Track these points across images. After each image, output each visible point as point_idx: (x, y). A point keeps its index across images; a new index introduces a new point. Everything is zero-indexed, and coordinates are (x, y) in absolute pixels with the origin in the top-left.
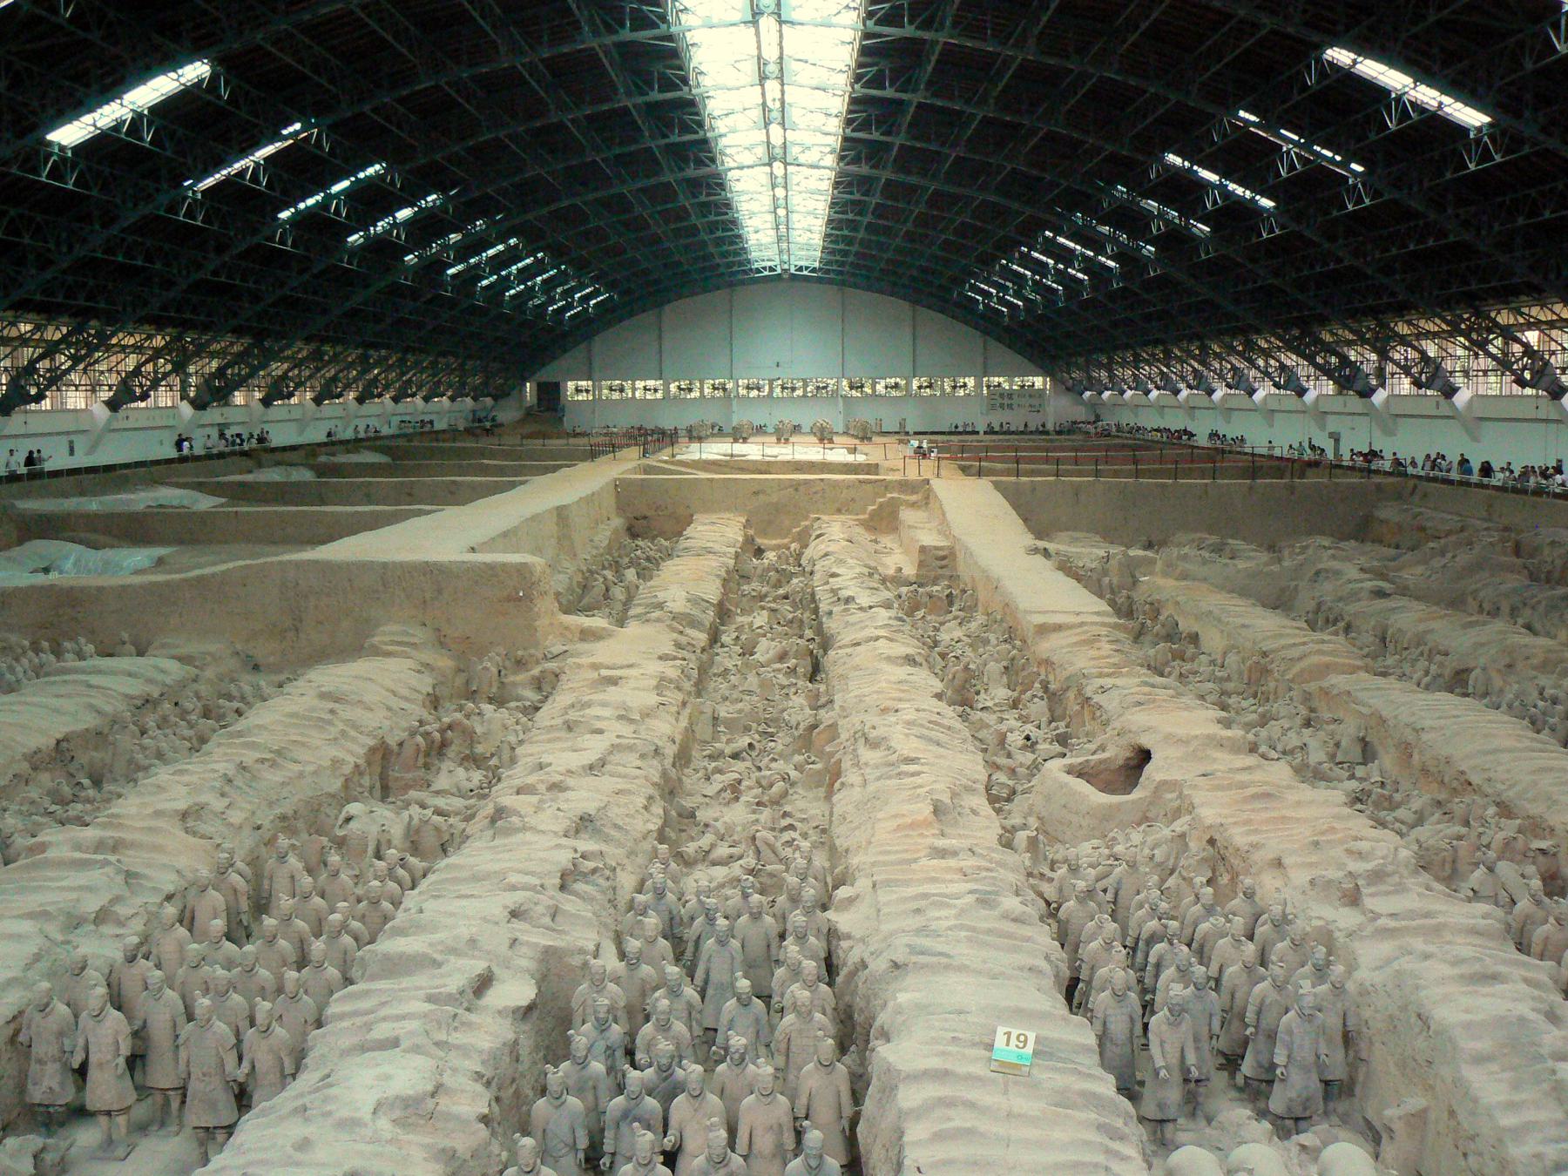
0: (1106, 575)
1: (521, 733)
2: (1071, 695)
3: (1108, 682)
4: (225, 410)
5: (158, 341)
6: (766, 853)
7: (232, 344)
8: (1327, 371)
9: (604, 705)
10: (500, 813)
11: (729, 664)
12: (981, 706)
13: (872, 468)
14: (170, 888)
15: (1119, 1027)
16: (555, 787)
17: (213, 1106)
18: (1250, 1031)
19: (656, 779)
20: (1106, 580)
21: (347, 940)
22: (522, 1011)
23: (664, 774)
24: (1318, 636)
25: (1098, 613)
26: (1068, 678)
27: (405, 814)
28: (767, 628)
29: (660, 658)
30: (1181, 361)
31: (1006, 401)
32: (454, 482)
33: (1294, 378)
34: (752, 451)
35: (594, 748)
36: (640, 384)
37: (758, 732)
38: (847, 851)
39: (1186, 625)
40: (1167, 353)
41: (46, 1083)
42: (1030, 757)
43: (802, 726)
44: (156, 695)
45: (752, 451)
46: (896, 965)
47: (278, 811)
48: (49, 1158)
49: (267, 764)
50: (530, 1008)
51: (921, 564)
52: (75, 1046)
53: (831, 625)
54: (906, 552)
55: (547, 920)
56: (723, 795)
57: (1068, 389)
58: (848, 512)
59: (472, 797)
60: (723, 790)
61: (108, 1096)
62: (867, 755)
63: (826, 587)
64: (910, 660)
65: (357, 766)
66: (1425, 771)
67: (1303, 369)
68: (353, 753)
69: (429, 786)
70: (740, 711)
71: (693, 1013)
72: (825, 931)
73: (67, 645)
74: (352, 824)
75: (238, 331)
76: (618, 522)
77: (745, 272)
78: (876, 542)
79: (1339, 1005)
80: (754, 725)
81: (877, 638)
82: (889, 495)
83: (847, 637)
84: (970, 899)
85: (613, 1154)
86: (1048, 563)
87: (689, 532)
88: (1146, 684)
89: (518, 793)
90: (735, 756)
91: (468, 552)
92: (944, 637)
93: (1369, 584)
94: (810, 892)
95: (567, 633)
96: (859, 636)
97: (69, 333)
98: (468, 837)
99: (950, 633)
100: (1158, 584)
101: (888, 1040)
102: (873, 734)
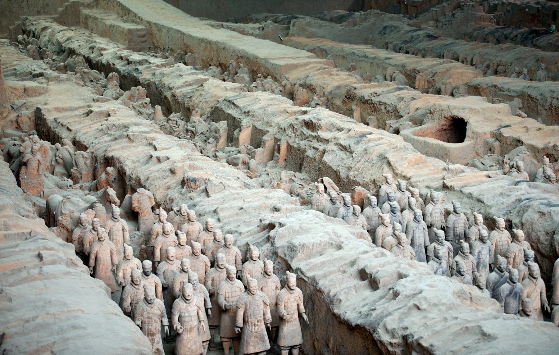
3: (378, 90)
17: (262, 338)
26: (330, 93)
43: (221, 131)
46: (543, 214)
51: (130, 41)
58: (46, 13)
61: (194, 347)
95: (16, 92)
102: (323, 123)
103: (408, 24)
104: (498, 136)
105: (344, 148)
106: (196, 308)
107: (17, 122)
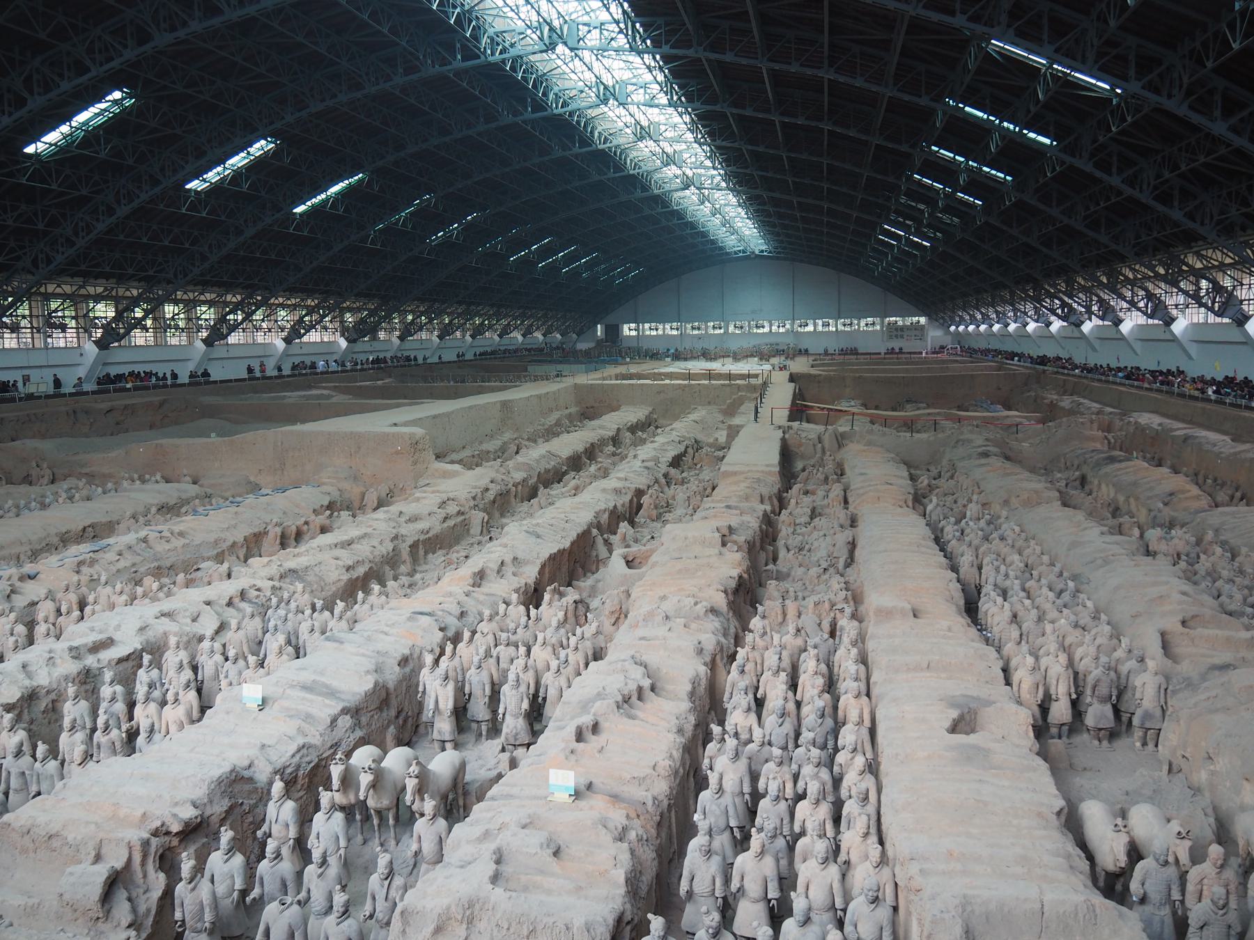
4: (375, 344)
25: (767, 466)
31: (899, 333)
36: (668, 326)
47: (156, 564)
49: (163, 541)
55: (189, 621)
65: (234, 543)
68: (239, 535)
75: (368, 295)
79: (557, 683)
91: (391, 426)
93: (980, 450)
97: (243, 300)
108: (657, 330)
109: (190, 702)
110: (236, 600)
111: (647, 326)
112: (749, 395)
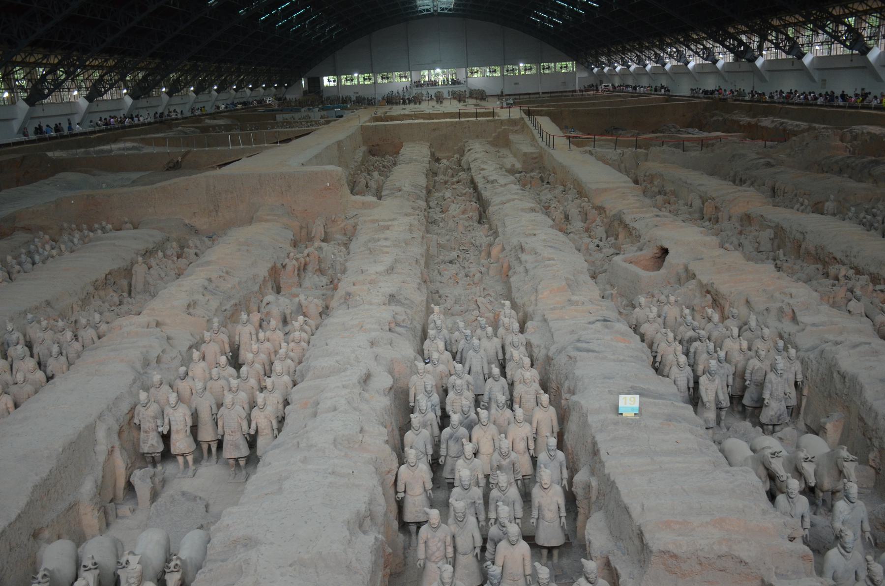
0: (622, 163)
1: (343, 256)
2: (616, 224)
5: (111, 63)
6: (482, 308)
7: (150, 63)
8: (731, 50)
9: (386, 239)
10: (349, 294)
11: (436, 217)
12: (569, 231)
13: (493, 114)
14: (188, 344)
15: (683, 383)
16: (372, 282)
17: (237, 447)
18: (748, 382)
19: (420, 275)
20: (623, 165)
21: (289, 361)
22: (388, 390)
23: (422, 273)
24: (740, 188)
27: (297, 300)
28: (453, 198)
29: (406, 215)
30: (648, 49)
32: (276, 132)
33: (711, 54)
34: (426, 107)
35: (388, 260)
37: (460, 250)
38: (524, 305)
39: (669, 188)
40: (641, 45)
41: (150, 442)
42: (600, 256)
44: (151, 246)
45: (426, 107)
46: (570, 357)
47: (232, 302)
48: (157, 480)
50: (391, 388)
52: (163, 423)
53: (486, 194)
54: (515, 156)
56: (450, 281)
57: (587, 68)
59: (324, 289)
60: (450, 278)
61: (181, 447)
62: (524, 257)
63: (480, 175)
64: (533, 210)
65: (265, 278)
66: (808, 253)
67: (719, 48)
68: (263, 271)
69: (301, 286)
70: (448, 241)
71: (470, 386)
72: (525, 344)
73: (96, 226)
74: (269, 306)
76: (364, 148)
77: (414, 13)
78: (498, 152)
80: (457, 247)
81: (513, 200)
82: (503, 127)
83: (496, 200)
84: (598, 324)
85: (445, 457)
86: (593, 158)
87: (402, 151)
88: (657, 216)
89: (354, 285)
90: (451, 262)
92: (543, 198)
94: (516, 326)
96: (504, 199)
97: (63, 59)
98: (333, 308)
99: (546, 195)
100: (653, 166)
101: (574, 394)
102: (526, 247)
103: (757, 153)
104: (687, 270)
105: (526, 271)
106: (181, 414)
107: (344, 229)
108: (370, 79)
109: (508, 418)
110: (393, 325)
111: (343, 77)
112: (512, 128)
